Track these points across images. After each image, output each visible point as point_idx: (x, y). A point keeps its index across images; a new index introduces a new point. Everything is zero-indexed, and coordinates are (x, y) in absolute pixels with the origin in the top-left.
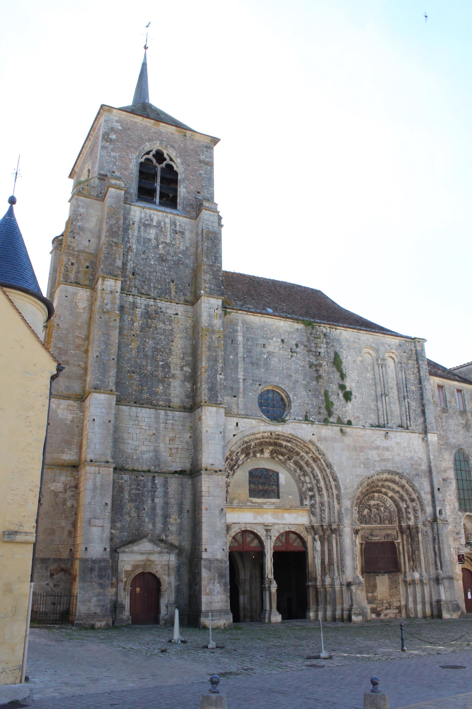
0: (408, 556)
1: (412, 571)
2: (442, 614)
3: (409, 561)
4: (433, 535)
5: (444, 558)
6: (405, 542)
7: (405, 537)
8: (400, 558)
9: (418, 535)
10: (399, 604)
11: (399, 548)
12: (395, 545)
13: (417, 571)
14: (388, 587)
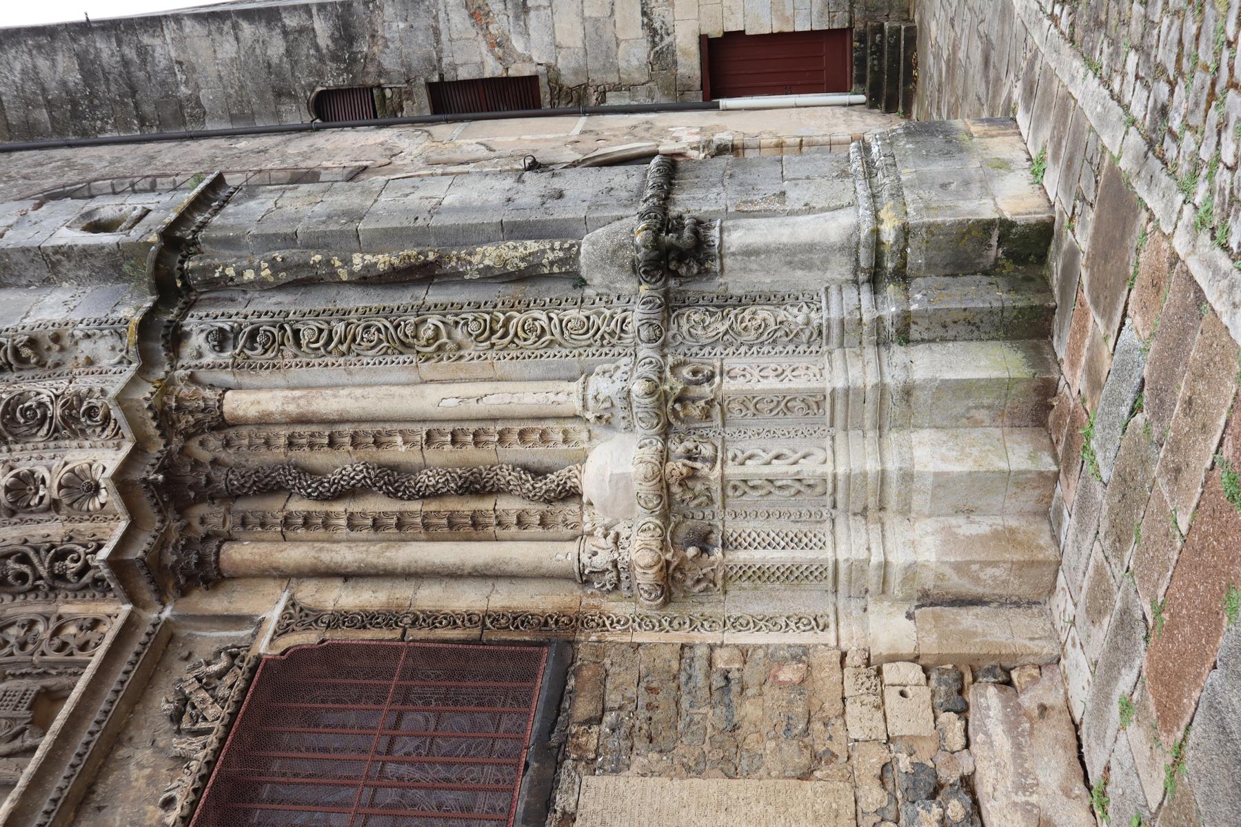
0: (429, 530)
1: (573, 506)
2: (1006, 226)
3: (475, 528)
4: (262, 286)
5: (482, 209)
6: (295, 554)
7: (241, 553)
8: (432, 619)
9: (237, 423)
10: (913, 673)
11: (341, 619)
12: (295, 656)
13: (582, 459)
14: (712, 786)
